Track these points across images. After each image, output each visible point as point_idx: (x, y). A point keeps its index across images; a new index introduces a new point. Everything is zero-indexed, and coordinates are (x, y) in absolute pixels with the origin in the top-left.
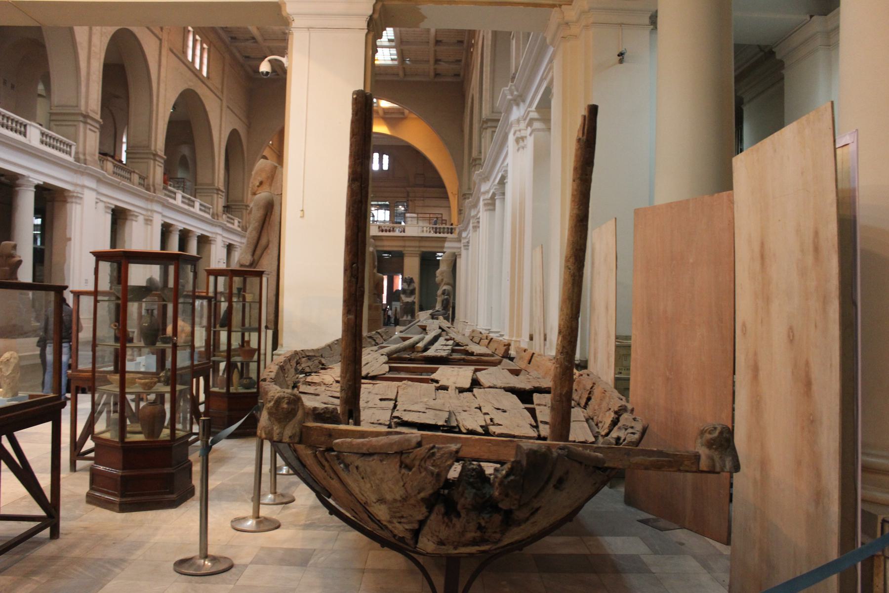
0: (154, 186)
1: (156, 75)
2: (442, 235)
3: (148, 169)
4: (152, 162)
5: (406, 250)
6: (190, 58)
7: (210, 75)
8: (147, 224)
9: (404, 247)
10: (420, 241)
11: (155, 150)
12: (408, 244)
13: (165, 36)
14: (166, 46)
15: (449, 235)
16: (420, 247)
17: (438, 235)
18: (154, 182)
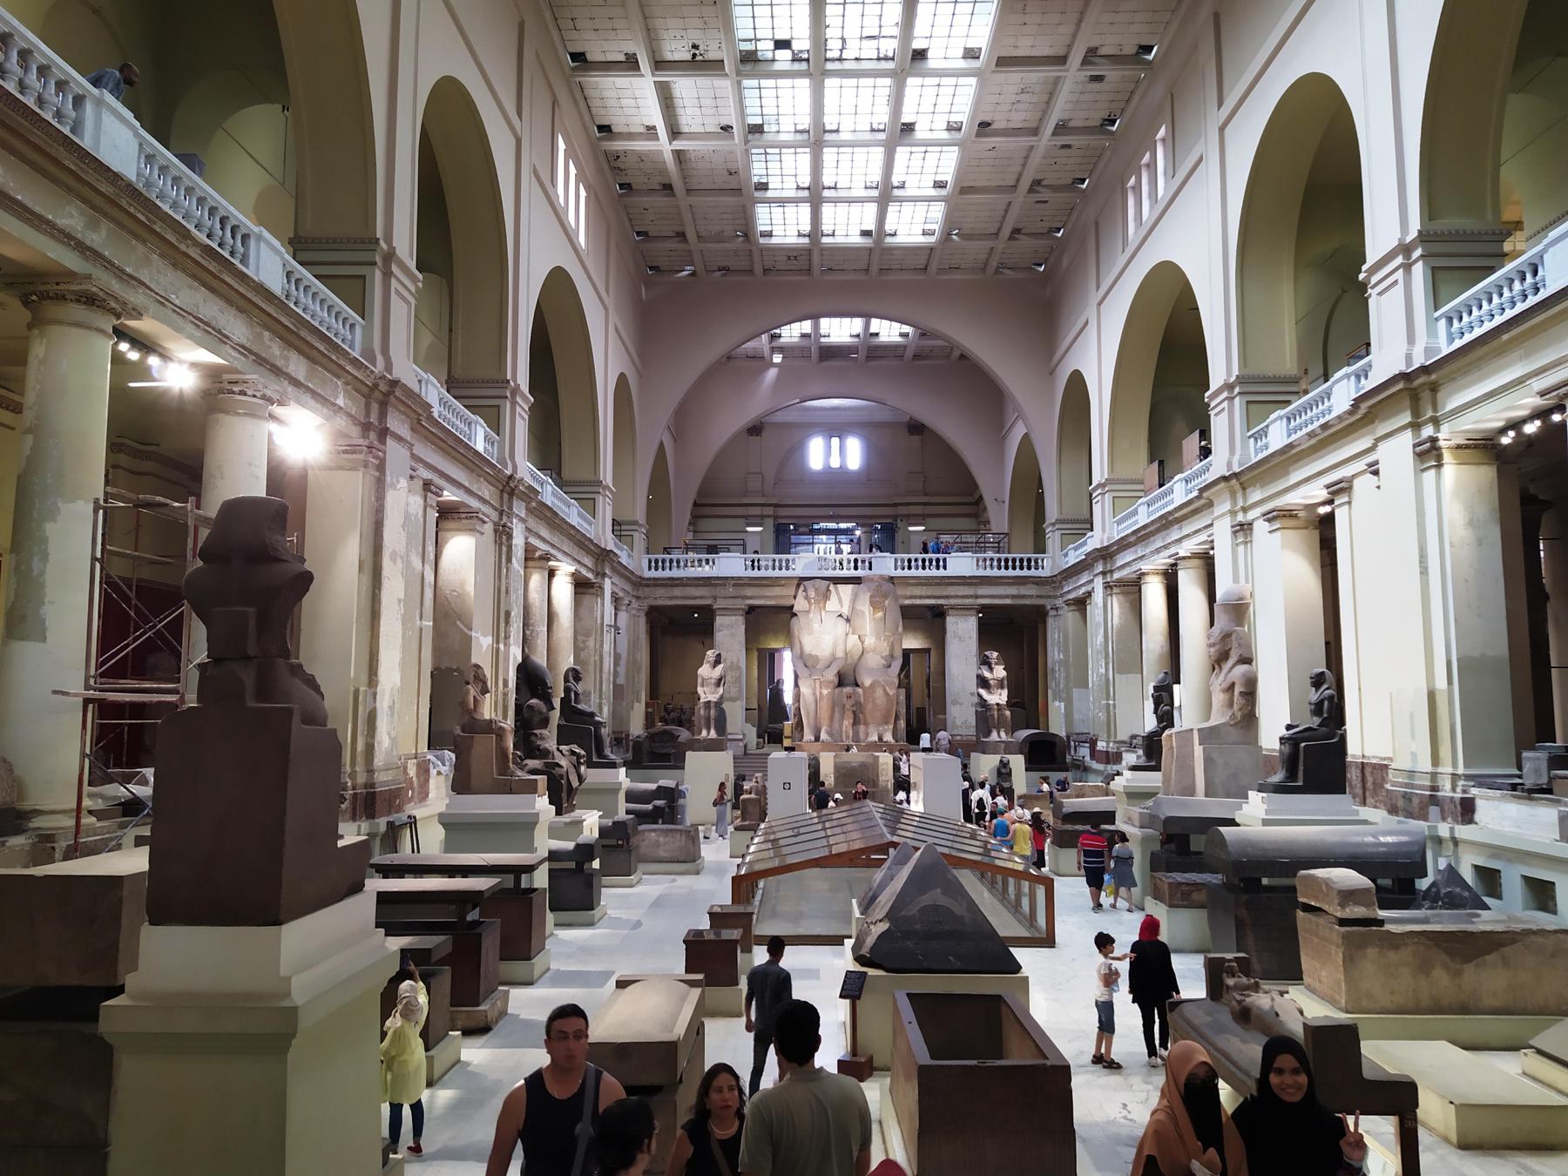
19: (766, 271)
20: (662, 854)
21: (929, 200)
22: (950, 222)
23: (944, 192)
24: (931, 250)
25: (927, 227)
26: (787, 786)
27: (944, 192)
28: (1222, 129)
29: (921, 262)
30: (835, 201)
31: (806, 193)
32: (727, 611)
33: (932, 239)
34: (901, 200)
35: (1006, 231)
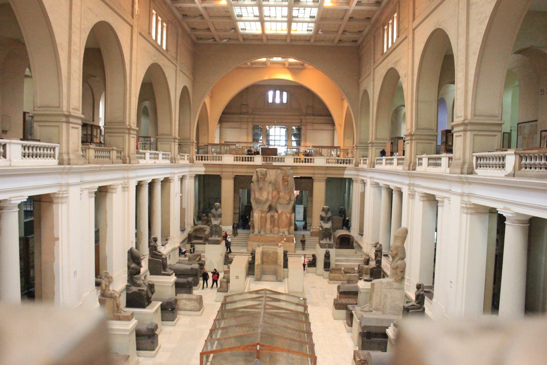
0: (129, 156)
1: (129, 58)
2: (342, 165)
3: (124, 142)
4: (127, 135)
5: (315, 177)
6: (154, 38)
7: (169, 49)
8: (124, 191)
9: (314, 174)
10: (326, 170)
11: (129, 125)
12: (316, 172)
13: (135, 23)
14: (136, 30)
15: (348, 165)
16: (325, 174)
17: (339, 165)
18: (129, 153)
19: (244, 39)
20: (187, 307)
21: (308, 22)
22: (317, 28)
23: (314, 20)
24: (311, 36)
25: (309, 29)
26: (237, 277)
27: (314, 20)
28: (414, 30)
29: (308, 38)
30: (271, 21)
31: (258, 19)
32: (227, 178)
33: (311, 33)
34: (297, 22)
35: (341, 31)
